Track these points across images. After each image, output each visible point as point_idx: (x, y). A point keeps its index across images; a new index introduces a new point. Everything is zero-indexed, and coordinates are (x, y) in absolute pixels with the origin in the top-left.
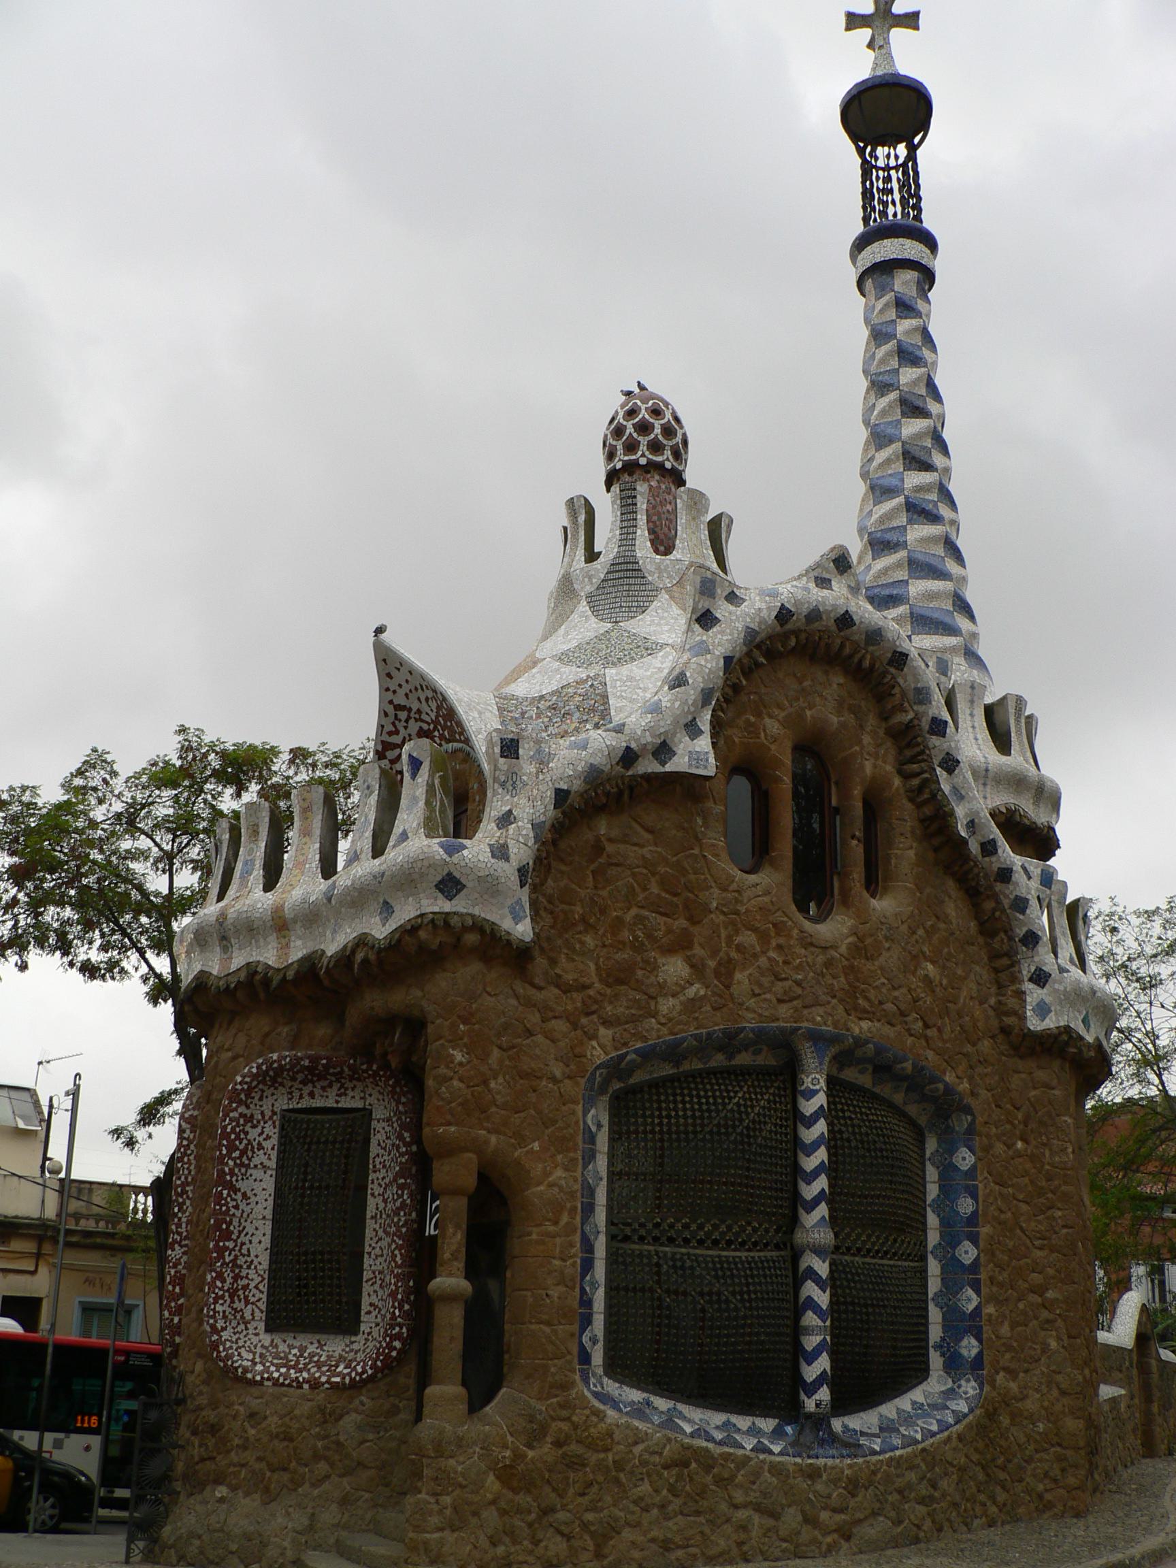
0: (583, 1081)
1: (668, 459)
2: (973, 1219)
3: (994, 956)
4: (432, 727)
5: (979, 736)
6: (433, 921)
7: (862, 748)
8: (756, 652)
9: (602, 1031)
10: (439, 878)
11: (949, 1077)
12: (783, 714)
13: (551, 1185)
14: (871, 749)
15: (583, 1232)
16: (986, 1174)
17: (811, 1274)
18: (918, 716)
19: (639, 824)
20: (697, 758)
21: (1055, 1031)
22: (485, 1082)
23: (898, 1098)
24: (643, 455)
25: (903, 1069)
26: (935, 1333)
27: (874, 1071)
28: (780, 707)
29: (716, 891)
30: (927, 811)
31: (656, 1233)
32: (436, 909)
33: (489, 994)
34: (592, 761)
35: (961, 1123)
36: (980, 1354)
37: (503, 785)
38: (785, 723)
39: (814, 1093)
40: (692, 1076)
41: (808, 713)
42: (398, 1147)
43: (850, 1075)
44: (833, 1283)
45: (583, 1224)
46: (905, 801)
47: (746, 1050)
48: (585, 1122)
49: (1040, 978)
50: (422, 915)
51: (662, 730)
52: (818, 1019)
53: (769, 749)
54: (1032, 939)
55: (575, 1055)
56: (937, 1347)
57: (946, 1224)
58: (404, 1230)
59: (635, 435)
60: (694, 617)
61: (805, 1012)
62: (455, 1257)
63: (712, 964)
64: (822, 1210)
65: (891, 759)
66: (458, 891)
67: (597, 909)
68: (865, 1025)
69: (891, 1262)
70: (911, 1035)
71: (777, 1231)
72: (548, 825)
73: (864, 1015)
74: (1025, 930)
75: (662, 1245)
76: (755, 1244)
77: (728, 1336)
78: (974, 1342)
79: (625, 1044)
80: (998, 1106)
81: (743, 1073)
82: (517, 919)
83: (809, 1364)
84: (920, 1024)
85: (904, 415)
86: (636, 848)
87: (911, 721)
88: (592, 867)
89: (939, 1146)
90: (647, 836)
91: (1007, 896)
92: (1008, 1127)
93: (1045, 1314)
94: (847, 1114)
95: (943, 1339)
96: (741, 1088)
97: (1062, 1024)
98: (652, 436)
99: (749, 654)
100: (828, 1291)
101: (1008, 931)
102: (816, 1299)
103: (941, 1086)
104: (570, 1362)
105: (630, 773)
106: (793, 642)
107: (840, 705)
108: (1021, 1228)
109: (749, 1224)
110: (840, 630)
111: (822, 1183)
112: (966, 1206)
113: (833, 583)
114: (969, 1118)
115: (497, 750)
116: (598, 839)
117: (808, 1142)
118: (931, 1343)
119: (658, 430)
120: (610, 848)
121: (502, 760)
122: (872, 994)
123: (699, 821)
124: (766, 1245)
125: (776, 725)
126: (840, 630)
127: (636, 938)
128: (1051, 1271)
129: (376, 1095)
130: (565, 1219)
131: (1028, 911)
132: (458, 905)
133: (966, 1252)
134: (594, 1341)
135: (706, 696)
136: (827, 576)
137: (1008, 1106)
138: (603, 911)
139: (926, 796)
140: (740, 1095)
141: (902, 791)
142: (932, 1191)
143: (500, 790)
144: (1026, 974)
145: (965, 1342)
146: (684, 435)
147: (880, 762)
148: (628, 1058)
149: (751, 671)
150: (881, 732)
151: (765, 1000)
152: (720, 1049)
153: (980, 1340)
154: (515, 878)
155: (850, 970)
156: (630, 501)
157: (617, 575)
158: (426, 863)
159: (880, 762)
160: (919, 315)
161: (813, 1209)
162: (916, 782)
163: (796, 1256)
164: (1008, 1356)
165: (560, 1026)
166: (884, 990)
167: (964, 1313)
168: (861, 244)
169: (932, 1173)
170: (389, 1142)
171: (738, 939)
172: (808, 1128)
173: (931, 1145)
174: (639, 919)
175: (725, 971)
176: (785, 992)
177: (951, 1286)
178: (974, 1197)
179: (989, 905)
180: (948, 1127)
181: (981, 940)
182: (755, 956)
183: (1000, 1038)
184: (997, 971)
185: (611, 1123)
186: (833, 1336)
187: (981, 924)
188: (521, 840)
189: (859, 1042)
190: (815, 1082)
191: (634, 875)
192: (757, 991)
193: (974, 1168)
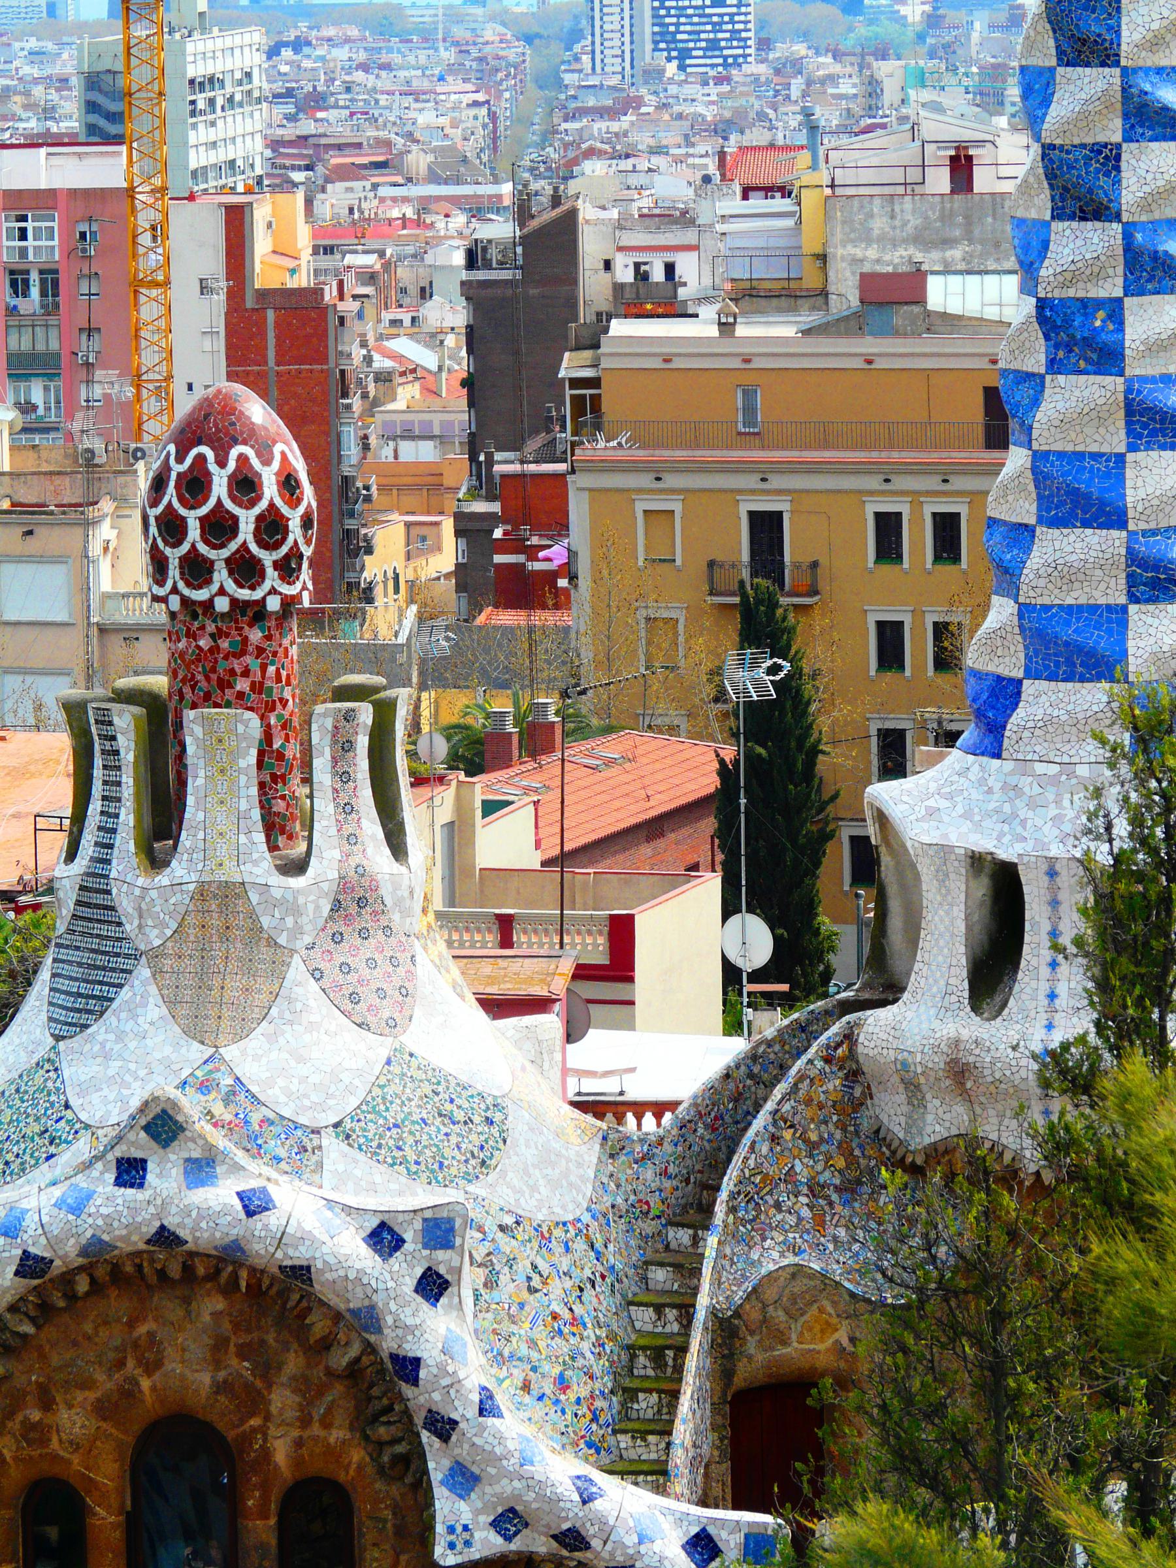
1: (222, 592)
5: (1062, 989)
7: (267, 1418)
12: (92, 1395)
18: (370, 1349)
24: (175, 590)
38: (102, 1410)
41: (145, 1384)
53: (69, 1462)
65: (341, 1418)
87: (357, 1360)
107: (219, 1345)
113: (150, 1166)
119: (194, 532)
136: (139, 1154)
147: (316, 1429)
159: (316, 1429)
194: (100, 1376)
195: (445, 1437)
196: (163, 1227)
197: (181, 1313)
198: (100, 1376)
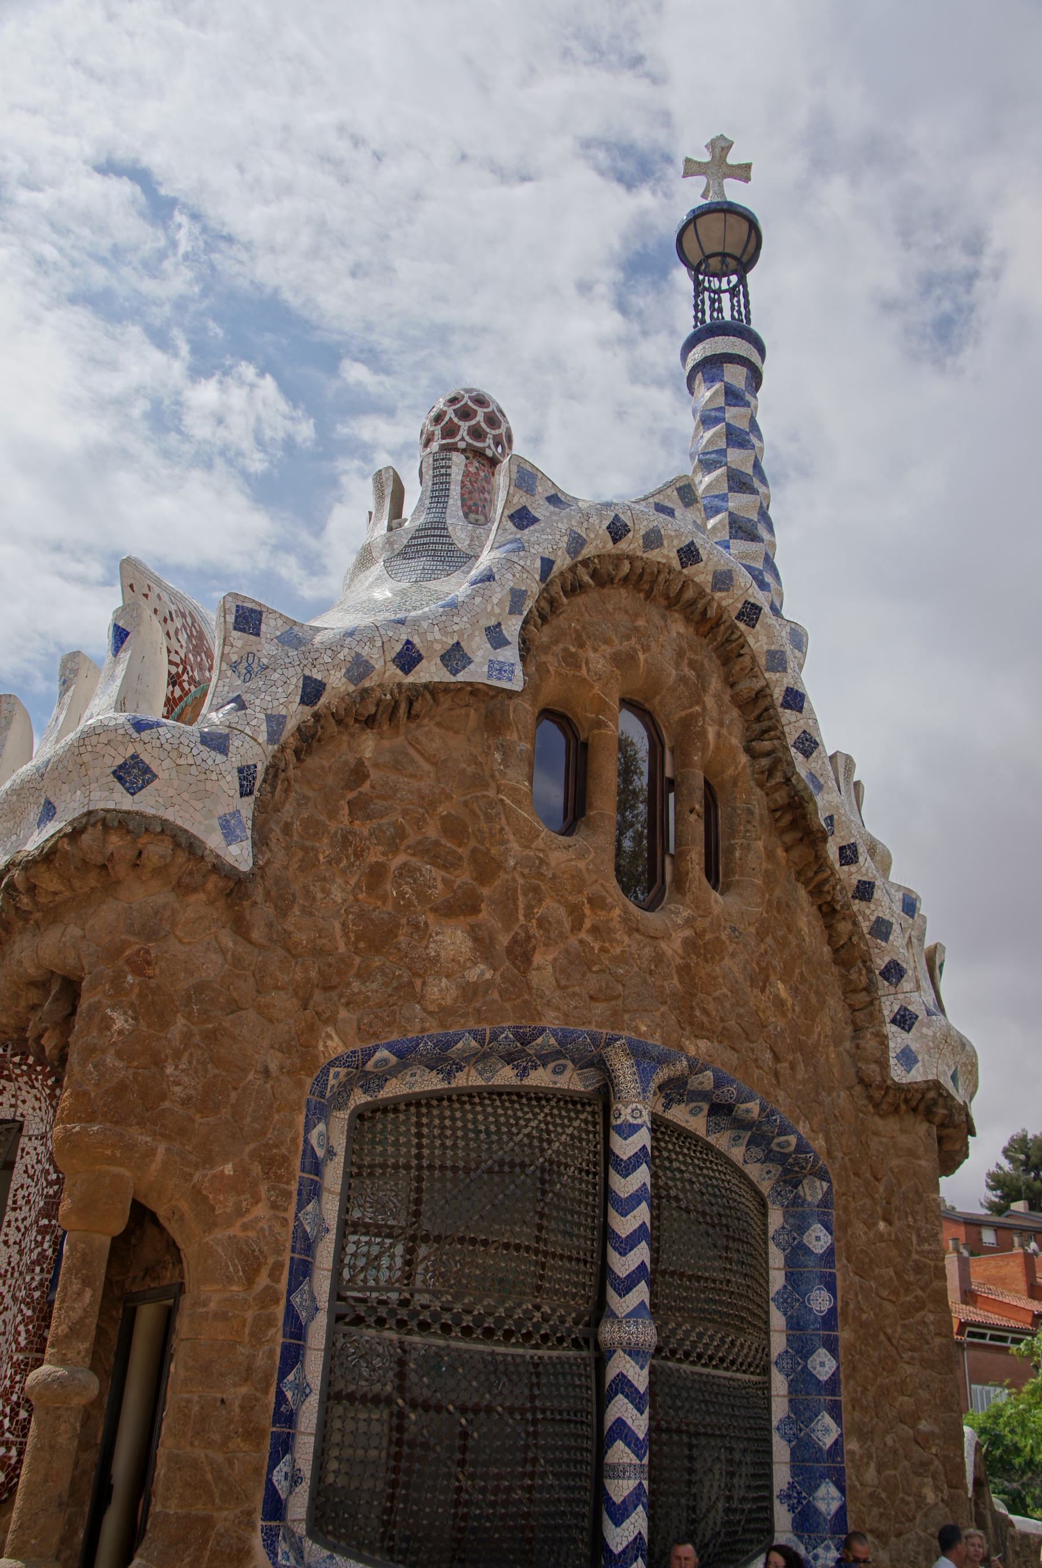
0: (309, 1082)
2: (830, 1319)
3: (849, 988)
4: (181, 668)
6: (104, 819)
7: (704, 708)
8: (581, 570)
9: (343, 1014)
10: (120, 761)
11: (803, 1128)
13: (245, 1227)
14: (715, 714)
15: (289, 1306)
16: (845, 1261)
17: (623, 1384)
19: (418, 751)
20: (498, 669)
21: (924, 1086)
22: (158, 1063)
23: (737, 1153)
24: (463, 439)
25: (748, 1111)
26: (782, 1476)
27: (710, 1113)
28: (607, 641)
29: (515, 846)
30: (781, 797)
31: (403, 1313)
32: (111, 805)
33: (180, 941)
34: (358, 649)
35: (813, 1191)
36: (842, 1510)
37: (234, 666)
39: (634, 1129)
40: (468, 1095)
41: (642, 657)
42: (47, 1172)
43: (679, 1114)
44: (650, 1400)
45: (290, 1292)
46: (752, 783)
47: (544, 1065)
48: (306, 1141)
49: (905, 1020)
50: (90, 813)
51: (456, 628)
52: (644, 1028)
54: (894, 972)
55: (301, 1048)
56: (786, 1497)
57: (795, 1324)
58: (37, 1294)
59: (456, 420)
60: (507, 513)
61: (626, 1017)
62: (75, 1331)
63: (504, 939)
64: (641, 1293)
66: (146, 783)
67: (350, 851)
68: (703, 1044)
69: (728, 1374)
70: (759, 1067)
71: (576, 1322)
72: (291, 725)
73: (700, 1031)
74: (887, 959)
75: (410, 1332)
76: (545, 1338)
77: (499, 1477)
78: (834, 1491)
79: (375, 1035)
80: (856, 1174)
81: (540, 1097)
82: (230, 835)
83: (618, 1523)
84: (768, 1055)
85: (731, 489)
86: (411, 780)
88: (351, 795)
89: (786, 1221)
90: (426, 766)
91: (866, 918)
92: (867, 1201)
93: (917, 1453)
94: (675, 1165)
95: (792, 1486)
96: (535, 1115)
97: (930, 1077)
98: (473, 422)
99: (572, 569)
100: (647, 1411)
101: (866, 960)
102: (629, 1422)
103: (793, 1139)
104: (249, 1513)
105: (410, 679)
106: (626, 567)
108: (885, 1333)
109: (538, 1308)
110: (684, 565)
111: (641, 1254)
112: (820, 1301)
114: (825, 1185)
115: (231, 619)
116: (360, 763)
117: (624, 1195)
118: (776, 1491)
119: (480, 417)
120: (374, 774)
121: (236, 634)
122: (711, 1007)
123: (498, 756)
124: (560, 1340)
125: (602, 661)
126: (684, 565)
127: (402, 895)
128: (924, 1394)
129: (31, 1102)
130: (263, 1280)
131: (891, 938)
132: (145, 803)
133: (822, 1364)
134: (295, 1479)
135: (517, 597)
136: (670, 505)
137: (868, 1175)
138: (358, 855)
139: (778, 780)
140: (534, 1124)
141: (748, 771)
142: (777, 1280)
143: (229, 673)
144: (887, 1013)
145: (821, 1492)
146: (508, 430)
148: (378, 1055)
149: (573, 590)
150: (727, 698)
151: (574, 994)
152: (509, 1059)
153: (842, 1490)
154: (231, 782)
155: (685, 971)
156: (443, 471)
157: (422, 541)
158: (103, 739)
160: (747, 404)
161: (628, 1290)
162: (765, 762)
163: (601, 1360)
164: (875, 1511)
165: (283, 1002)
166: (727, 1005)
167: (821, 1449)
168: (691, 343)
169: (776, 1258)
170: (39, 1167)
171: (539, 911)
172: (625, 1176)
173: (776, 1218)
174: (406, 870)
175: (521, 954)
176: (600, 990)
177: (802, 1412)
178: (831, 1288)
179: (844, 927)
180: (797, 1196)
181: (835, 969)
182: (562, 936)
183: (858, 1088)
184: (853, 1009)
185: (350, 1151)
186: (651, 1480)
187: (836, 951)
188: (248, 730)
189: (695, 1067)
190: (637, 1114)
191: (405, 813)
192: (563, 983)
193: (830, 1252)
194: (616, 641)
195: (807, 754)
196: (692, 543)
197: (662, 623)
198: (616, 641)
